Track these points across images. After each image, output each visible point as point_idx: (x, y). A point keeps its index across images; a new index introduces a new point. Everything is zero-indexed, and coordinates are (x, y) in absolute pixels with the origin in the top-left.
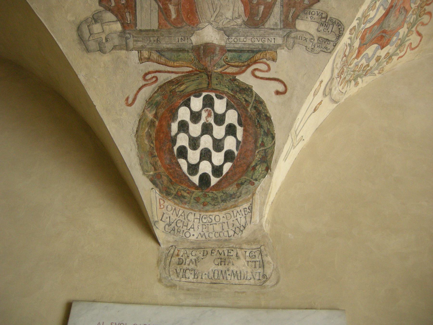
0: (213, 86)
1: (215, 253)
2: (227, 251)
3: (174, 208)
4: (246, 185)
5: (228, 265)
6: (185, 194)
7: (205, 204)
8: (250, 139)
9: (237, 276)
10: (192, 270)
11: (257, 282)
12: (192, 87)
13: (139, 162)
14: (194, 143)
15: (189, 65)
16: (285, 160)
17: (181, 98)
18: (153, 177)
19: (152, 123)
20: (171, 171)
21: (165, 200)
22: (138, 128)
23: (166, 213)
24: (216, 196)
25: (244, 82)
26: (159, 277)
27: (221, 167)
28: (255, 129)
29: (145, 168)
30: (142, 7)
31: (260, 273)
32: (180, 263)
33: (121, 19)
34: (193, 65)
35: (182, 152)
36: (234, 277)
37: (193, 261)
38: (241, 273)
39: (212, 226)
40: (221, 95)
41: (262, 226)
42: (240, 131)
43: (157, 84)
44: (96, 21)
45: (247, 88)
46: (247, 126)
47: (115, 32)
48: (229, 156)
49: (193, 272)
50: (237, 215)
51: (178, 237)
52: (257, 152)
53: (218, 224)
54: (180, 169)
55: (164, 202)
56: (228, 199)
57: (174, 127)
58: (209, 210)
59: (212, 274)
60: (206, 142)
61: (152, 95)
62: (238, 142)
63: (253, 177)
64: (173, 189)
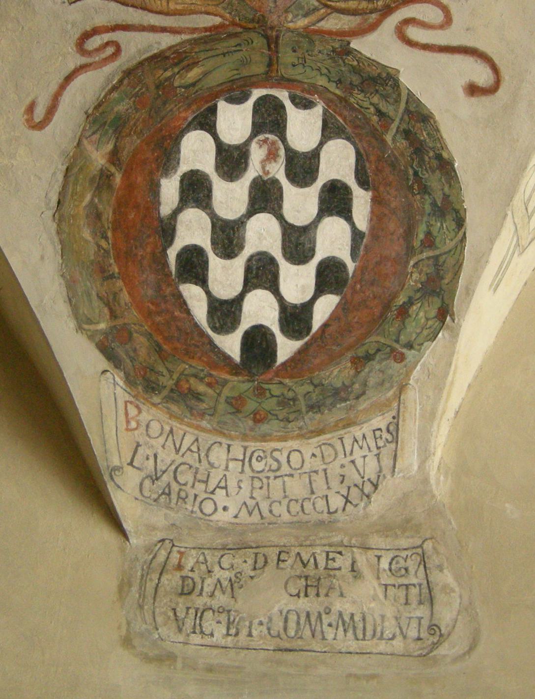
0: (283, 71)
1: (290, 562)
2: (324, 555)
3: (167, 428)
4: (380, 362)
5: (327, 595)
6: (202, 388)
7: (258, 418)
8: (392, 226)
9: (355, 628)
10: (222, 610)
11: (412, 645)
12: (222, 73)
13: (65, 293)
14: (228, 238)
15: (211, 9)
17: (189, 106)
18: (106, 338)
19: (103, 180)
20: (158, 319)
21: (141, 406)
22: (62, 194)
23: (146, 444)
24: (291, 395)
25: (373, 57)
26: (124, 631)
28: (406, 197)
29: (84, 310)
31: (420, 619)
32: (187, 590)
34: (225, 9)
35: (193, 265)
36: (345, 631)
37: (225, 583)
38: (364, 619)
39: (279, 481)
40: (307, 96)
41: (426, 481)
42: (361, 202)
43: (117, 63)
45: (384, 75)
46: (382, 189)
48: (330, 276)
49: (223, 618)
50: (353, 449)
51: (180, 515)
52: (412, 263)
53: (296, 476)
54: (185, 315)
55: (140, 411)
56: (329, 401)
57: (170, 190)
58: (270, 435)
59: (281, 624)
60: (263, 234)
61: (105, 97)
62: (357, 236)
63: (402, 337)
64: (165, 372)
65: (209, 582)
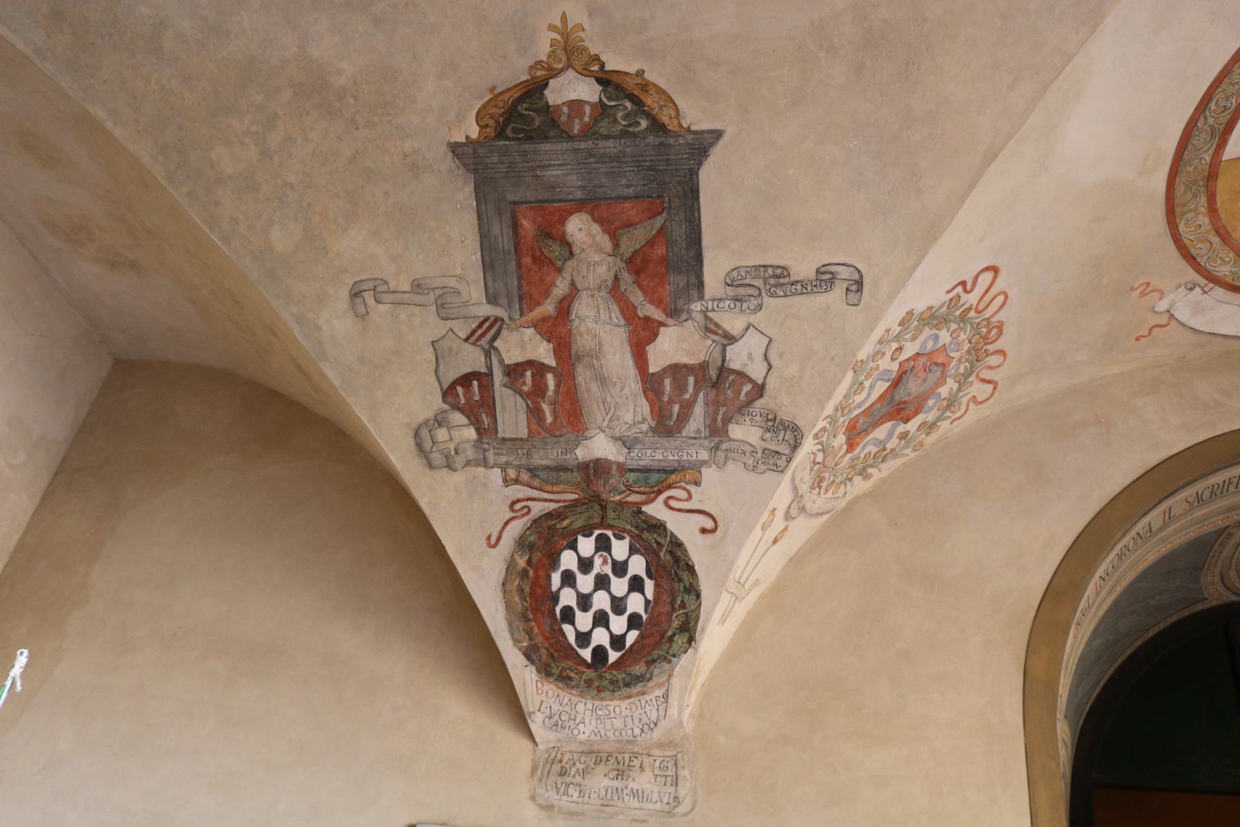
6: (572, 675)
7: (599, 689)
12: (578, 524)
14: (584, 602)
16: (723, 621)
19: (524, 573)
22: (506, 579)
27: (623, 637)
29: (517, 636)
30: (503, 406)
32: (562, 774)
33: (475, 421)
35: (568, 615)
41: (681, 723)
42: (649, 585)
44: (440, 425)
47: (468, 441)
48: (634, 621)
57: (556, 579)
60: (601, 601)
62: (647, 602)
65: (574, 769)
